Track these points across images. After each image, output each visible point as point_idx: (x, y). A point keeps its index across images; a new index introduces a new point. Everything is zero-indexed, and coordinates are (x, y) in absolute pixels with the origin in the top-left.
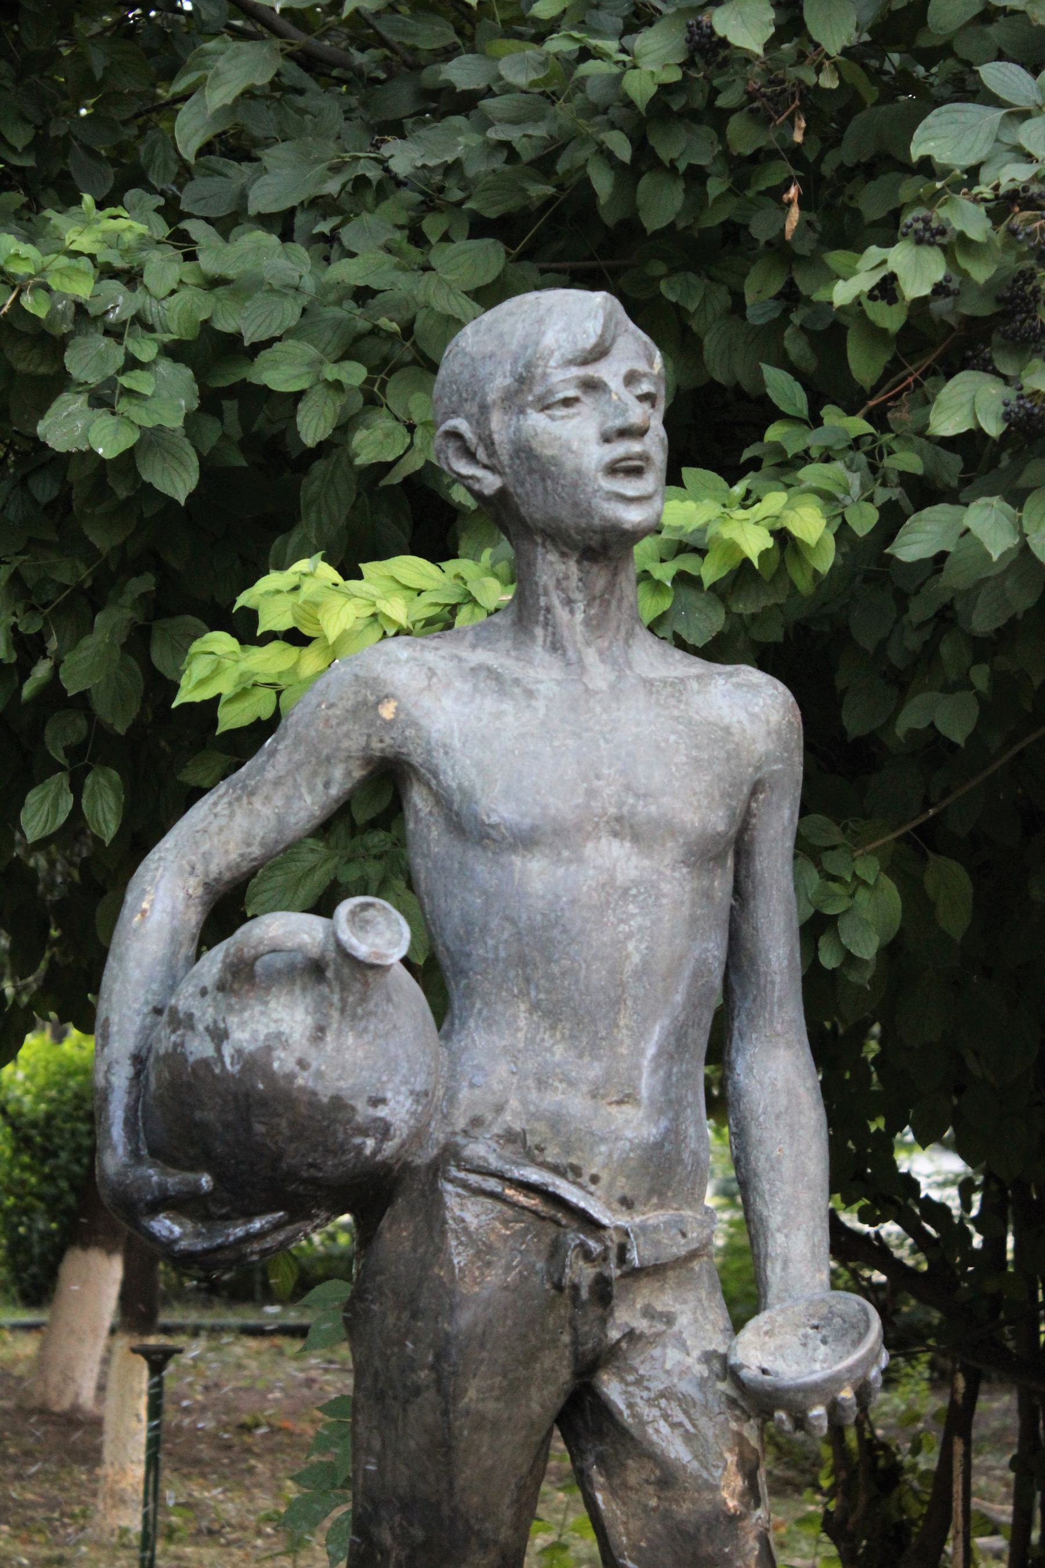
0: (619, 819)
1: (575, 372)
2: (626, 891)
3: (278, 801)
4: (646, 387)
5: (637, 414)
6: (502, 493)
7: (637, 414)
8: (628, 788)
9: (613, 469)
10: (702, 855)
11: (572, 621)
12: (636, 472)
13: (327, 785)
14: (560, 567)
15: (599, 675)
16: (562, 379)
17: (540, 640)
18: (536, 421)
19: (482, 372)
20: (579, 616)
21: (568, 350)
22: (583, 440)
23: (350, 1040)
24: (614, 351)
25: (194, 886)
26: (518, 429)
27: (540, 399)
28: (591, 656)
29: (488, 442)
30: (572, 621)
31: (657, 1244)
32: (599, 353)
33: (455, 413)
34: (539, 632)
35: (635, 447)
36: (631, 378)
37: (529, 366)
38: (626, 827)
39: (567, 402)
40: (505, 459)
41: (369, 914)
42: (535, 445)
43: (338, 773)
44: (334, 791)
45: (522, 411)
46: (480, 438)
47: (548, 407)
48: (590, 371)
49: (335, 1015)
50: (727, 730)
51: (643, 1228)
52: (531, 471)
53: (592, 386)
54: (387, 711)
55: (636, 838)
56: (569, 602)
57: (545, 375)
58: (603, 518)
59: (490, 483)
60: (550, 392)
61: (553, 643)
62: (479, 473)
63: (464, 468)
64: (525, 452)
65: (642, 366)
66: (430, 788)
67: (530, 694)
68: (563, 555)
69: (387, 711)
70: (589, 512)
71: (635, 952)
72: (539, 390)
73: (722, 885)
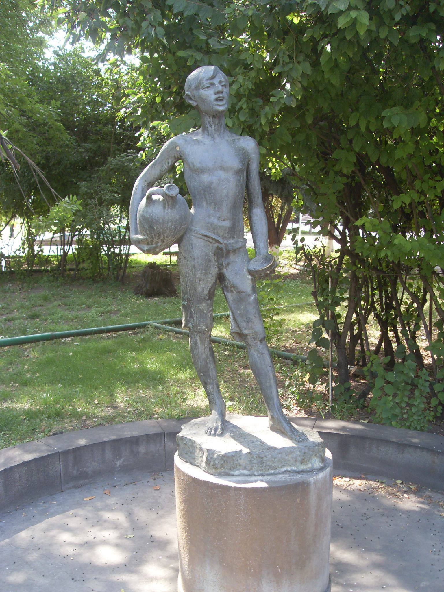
0: (221, 167)
1: (208, 81)
2: (223, 180)
3: (160, 167)
4: (223, 84)
5: (220, 88)
6: (197, 105)
7: (220, 88)
8: (222, 161)
9: (217, 100)
10: (238, 172)
11: (212, 129)
12: (222, 100)
13: (168, 163)
14: (209, 119)
15: (218, 140)
16: (206, 83)
18: (202, 92)
20: (213, 128)
21: (207, 77)
22: (211, 95)
23: (170, 210)
24: (217, 77)
25: (146, 184)
28: (216, 136)
30: (212, 129)
31: (233, 246)
32: (213, 78)
34: (206, 132)
35: (221, 95)
36: (220, 82)
38: (222, 168)
39: (207, 87)
41: (171, 187)
42: (202, 96)
43: (170, 161)
44: (170, 164)
45: (199, 90)
48: (211, 81)
49: (167, 206)
50: (243, 149)
51: (230, 243)
53: (212, 84)
54: (178, 149)
55: (224, 170)
56: (211, 126)
57: (203, 83)
60: (204, 86)
63: (190, 102)
64: (200, 97)
65: (223, 79)
67: (204, 144)
69: (178, 149)
70: (212, 108)
71: (225, 192)
72: (202, 85)
73: (243, 178)
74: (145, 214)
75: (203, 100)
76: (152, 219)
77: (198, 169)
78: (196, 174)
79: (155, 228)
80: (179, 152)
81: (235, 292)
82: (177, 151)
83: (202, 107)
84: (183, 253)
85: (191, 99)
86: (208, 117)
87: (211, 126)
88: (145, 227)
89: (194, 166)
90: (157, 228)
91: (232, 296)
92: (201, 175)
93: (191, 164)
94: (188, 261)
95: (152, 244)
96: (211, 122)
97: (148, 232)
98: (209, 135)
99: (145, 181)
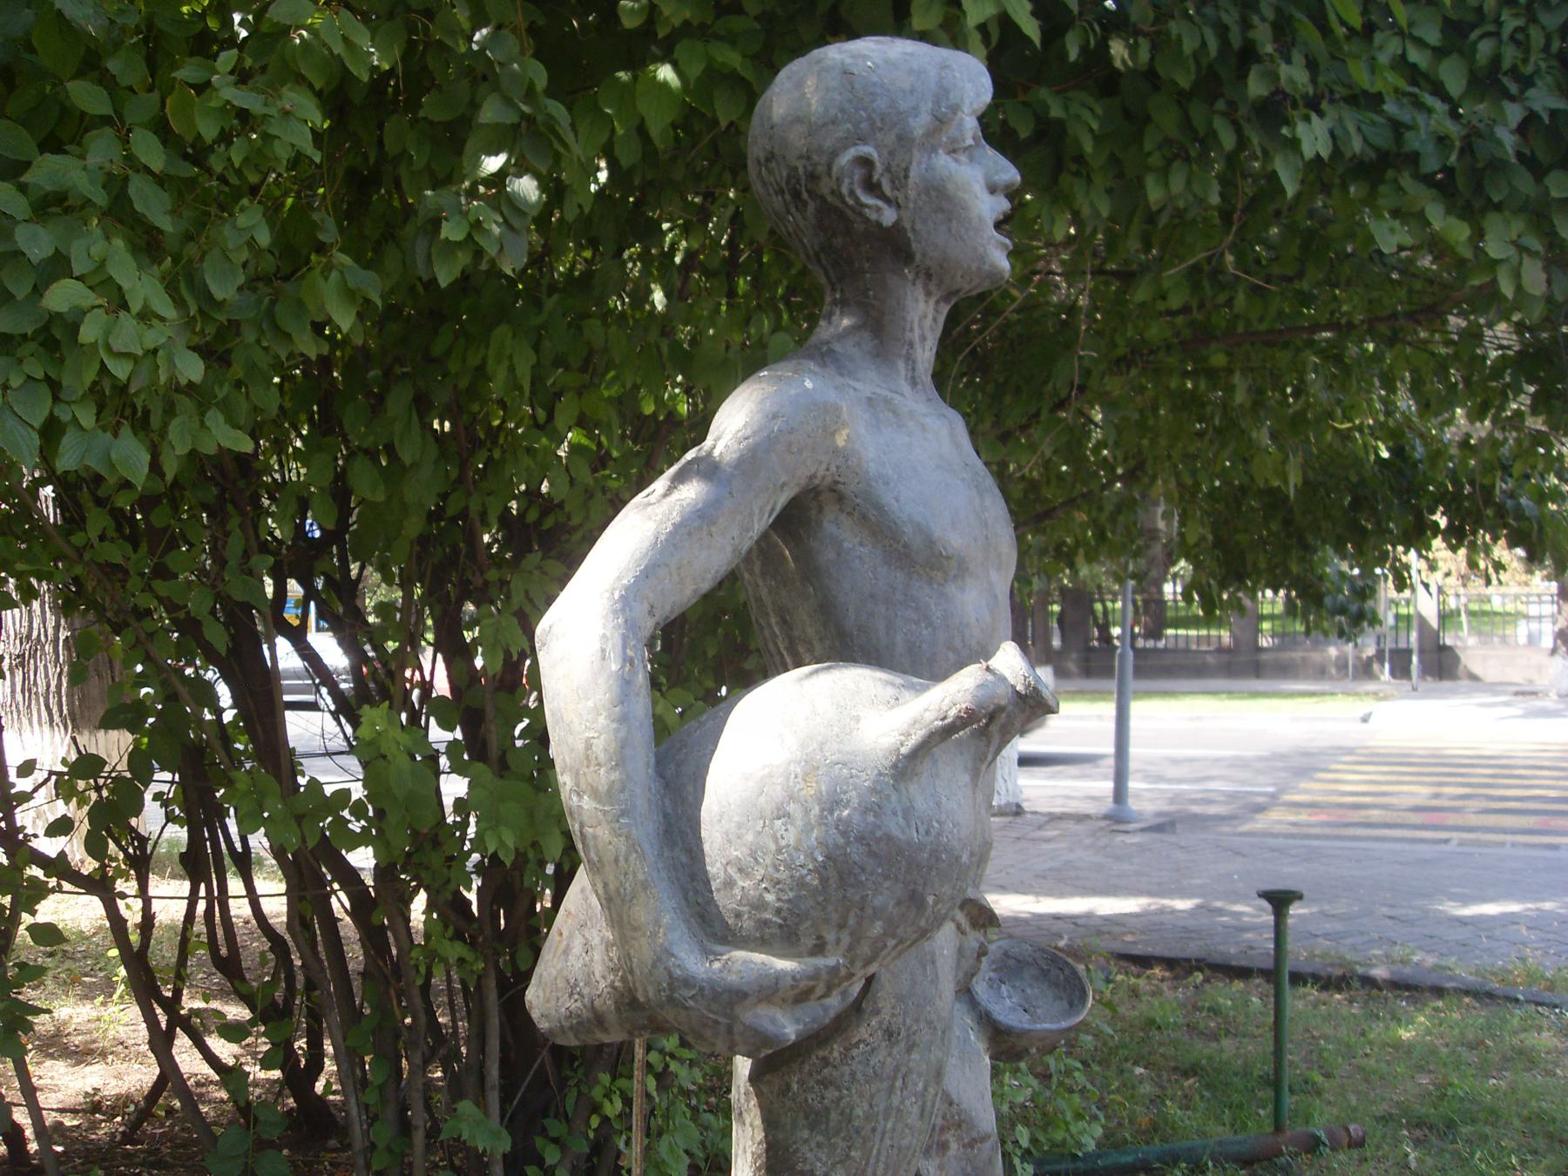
14: (922, 306)
17: (903, 372)
18: (943, 161)
19: (903, 105)
26: (930, 168)
27: (953, 140)
29: (900, 178)
33: (862, 140)
34: (901, 365)
37: (955, 109)
40: (912, 194)
42: (950, 187)
45: (934, 150)
46: (888, 169)
47: (954, 151)
52: (940, 209)
58: (993, 265)
59: (889, 216)
61: (913, 378)
62: (880, 203)
66: (864, 517)
67: (923, 428)
68: (928, 294)
69: (840, 441)
70: (982, 259)
74: (894, 826)
75: (941, 198)
76: (935, 854)
77: (948, 558)
78: (930, 582)
79: (930, 899)
80: (843, 455)
81: (954, 1146)
82: (836, 451)
83: (930, 240)
84: (886, 1016)
85: (872, 187)
86: (919, 292)
87: (923, 339)
88: (878, 901)
89: (930, 543)
90: (936, 903)
91: (941, 1167)
92: (951, 589)
93: (908, 529)
94: (909, 1049)
95: (827, 995)
96: (928, 322)
97: (877, 928)
98: (914, 382)
99: (651, 613)
